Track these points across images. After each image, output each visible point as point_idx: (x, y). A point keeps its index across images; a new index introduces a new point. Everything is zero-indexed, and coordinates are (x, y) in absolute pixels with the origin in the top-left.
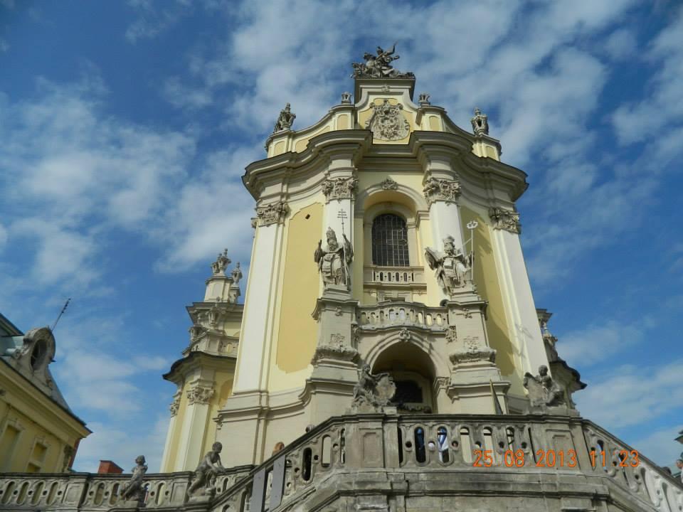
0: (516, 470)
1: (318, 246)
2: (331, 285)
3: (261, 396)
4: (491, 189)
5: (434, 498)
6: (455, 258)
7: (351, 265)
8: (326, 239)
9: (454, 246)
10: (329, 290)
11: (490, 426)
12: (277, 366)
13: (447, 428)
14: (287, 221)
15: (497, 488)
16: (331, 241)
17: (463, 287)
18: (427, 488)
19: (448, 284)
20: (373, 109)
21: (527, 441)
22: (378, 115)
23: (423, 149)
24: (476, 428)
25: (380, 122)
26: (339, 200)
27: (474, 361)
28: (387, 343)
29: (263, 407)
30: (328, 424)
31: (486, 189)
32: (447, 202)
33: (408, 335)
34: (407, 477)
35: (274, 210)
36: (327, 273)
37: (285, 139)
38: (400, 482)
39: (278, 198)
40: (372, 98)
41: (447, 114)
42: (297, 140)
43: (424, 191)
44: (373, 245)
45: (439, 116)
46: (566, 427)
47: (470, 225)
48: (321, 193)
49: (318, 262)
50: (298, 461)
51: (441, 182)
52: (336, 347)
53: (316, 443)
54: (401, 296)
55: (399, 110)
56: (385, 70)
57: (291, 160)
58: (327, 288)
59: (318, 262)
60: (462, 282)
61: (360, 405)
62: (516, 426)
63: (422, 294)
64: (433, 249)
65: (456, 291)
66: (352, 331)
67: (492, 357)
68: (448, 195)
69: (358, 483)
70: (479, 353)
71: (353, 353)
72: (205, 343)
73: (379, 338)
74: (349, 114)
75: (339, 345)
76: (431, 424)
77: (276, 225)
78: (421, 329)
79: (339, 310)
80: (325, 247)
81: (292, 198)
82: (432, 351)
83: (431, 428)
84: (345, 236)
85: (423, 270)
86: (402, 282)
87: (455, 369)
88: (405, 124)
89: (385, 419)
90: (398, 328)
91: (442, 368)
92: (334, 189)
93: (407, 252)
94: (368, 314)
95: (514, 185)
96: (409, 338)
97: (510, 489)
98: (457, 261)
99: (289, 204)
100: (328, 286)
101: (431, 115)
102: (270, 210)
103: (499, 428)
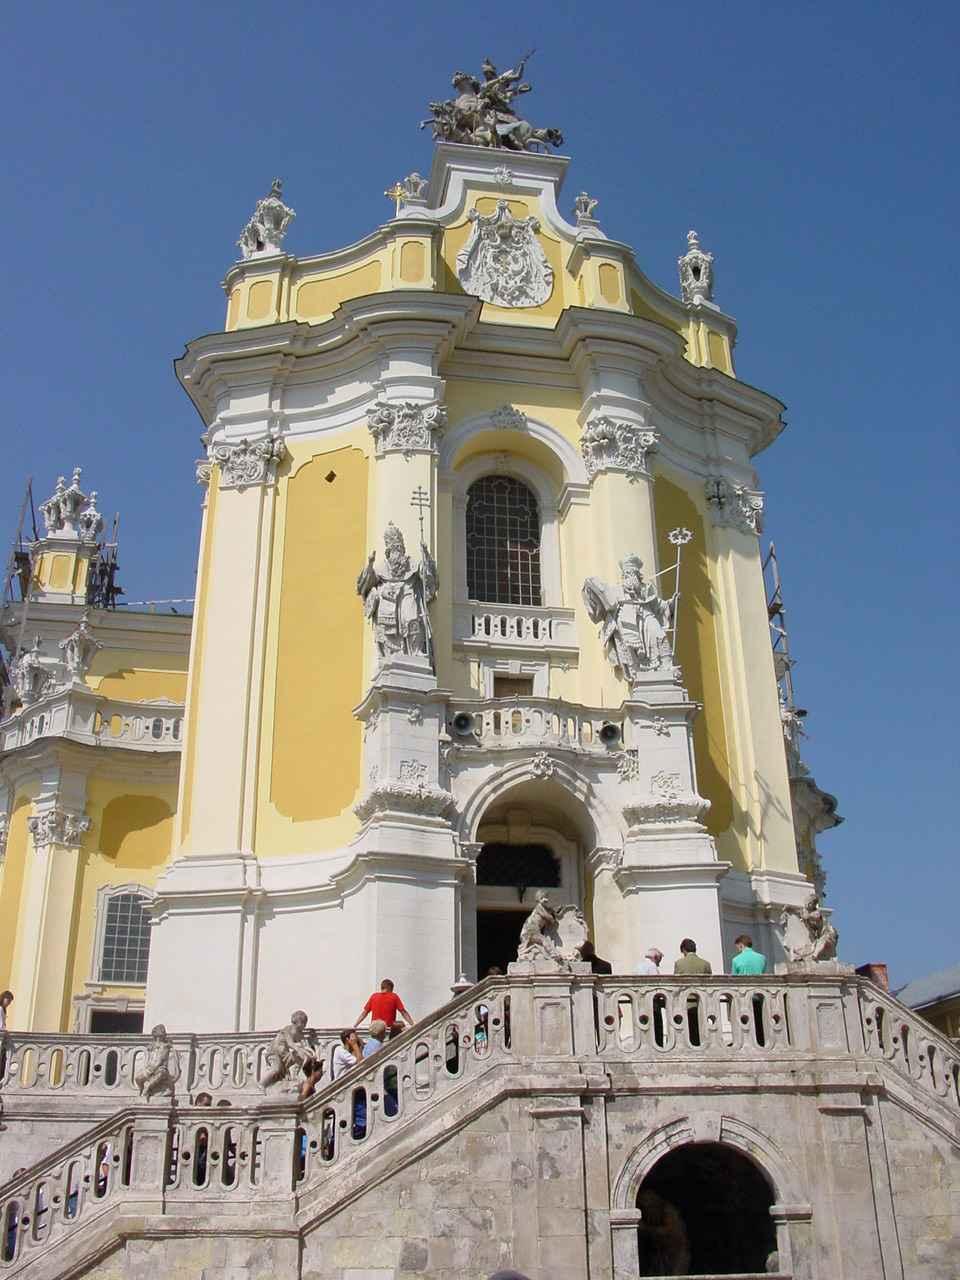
1: (368, 563)
2: (398, 657)
3: (245, 866)
6: (641, 605)
7: (432, 606)
12: (273, 805)
16: (394, 555)
17: (656, 669)
19: (626, 658)
21: (782, 1014)
23: (586, 347)
25: (490, 260)
26: (408, 453)
27: (670, 821)
28: (507, 781)
29: (251, 892)
32: (629, 474)
33: (548, 767)
35: (253, 452)
36: (388, 627)
37: (275, 277)
39: (264, 424)
45: (619, 266)
49: (366, 595)
50: (440, 1047)
51: (620, 427)
52: (411, 787)
54: (527, 670)
55: (532, 233)
57: (294, 339)
58: (385, 661)
60: (654, 657)
63: (568, 668)
65: (641, 677)
66: (441, 754)
67: (704, 816)
68: (632, 459)
70: (679, 805)
71: (445, 800)
72: (63, 714)
73: (491, 769)
74: (427, 242)
76: (643, 990)
78: (573, 752)
79: (416, 711)
80: (381, 567)
81: (294, 427)
82: (591, 798)
84: (425, 548)
85: (572, 615)
86: (528, 640)
87: (632, 834)
88: (545, 271)
90: (530, 751)
91: (609, 833)
92: (395, 427)
93: (536, 568)
95: (759, 428)
96: (550, 772)
98: (646, 613)
100: (390, 659)
101: (605, 261)
102: (244, 451)
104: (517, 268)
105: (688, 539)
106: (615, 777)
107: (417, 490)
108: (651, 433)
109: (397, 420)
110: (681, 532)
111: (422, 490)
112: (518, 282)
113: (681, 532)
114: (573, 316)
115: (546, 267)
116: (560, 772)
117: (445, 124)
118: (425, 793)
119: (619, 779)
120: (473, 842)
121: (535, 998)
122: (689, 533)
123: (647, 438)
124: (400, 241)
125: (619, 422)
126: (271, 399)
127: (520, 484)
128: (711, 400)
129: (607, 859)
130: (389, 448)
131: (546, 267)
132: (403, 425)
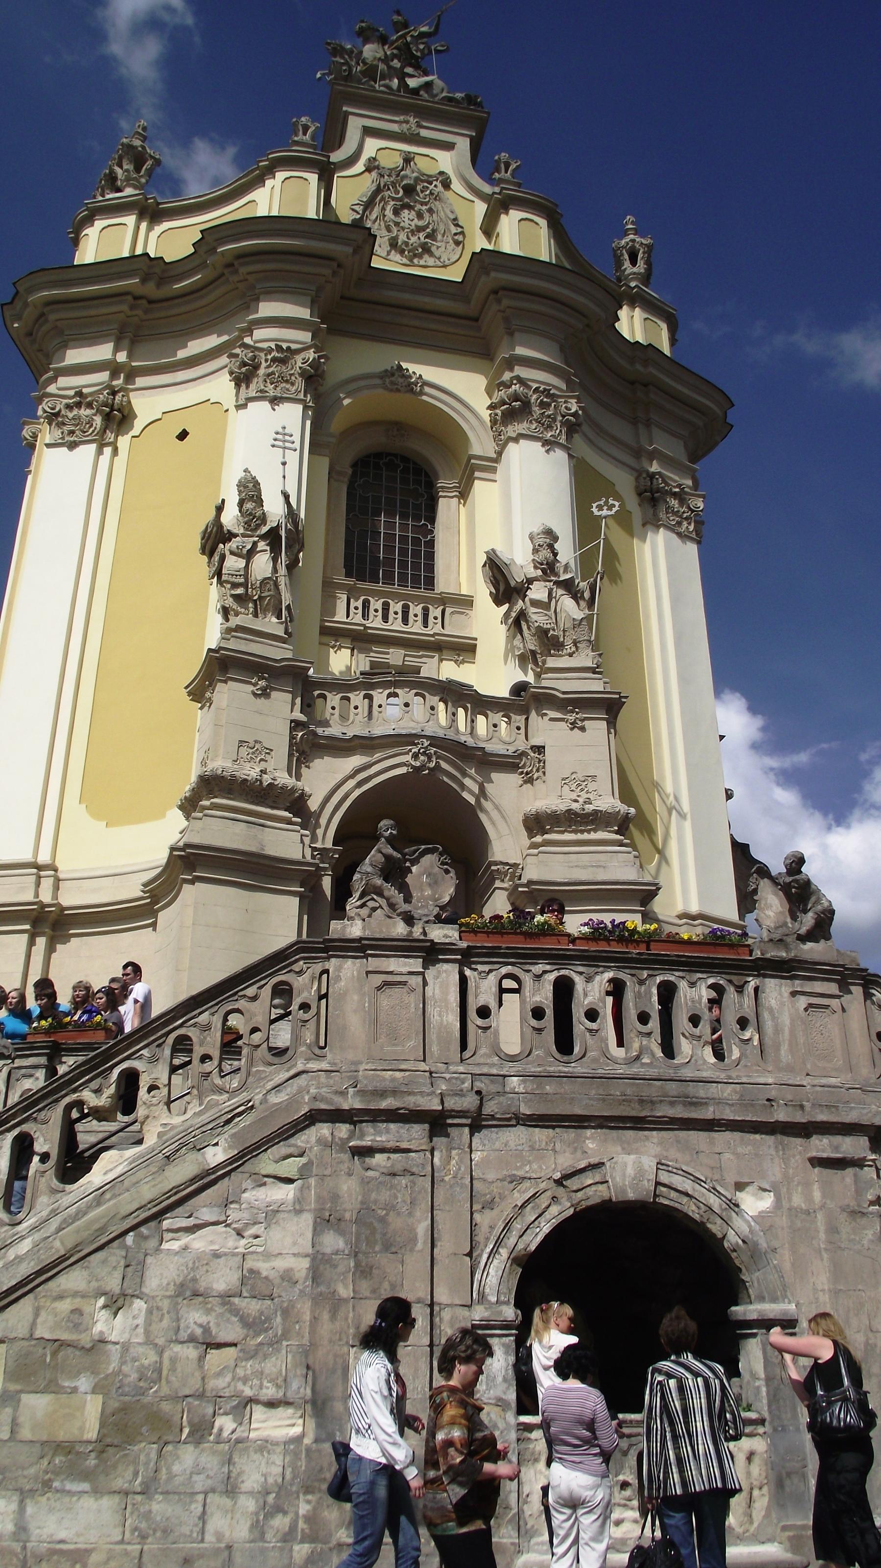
0: (722, 1076)
1: (214, 513)
2: (244, 619)
4: (648, 424)
5: (537, 1130)
6: (556, 583)
7: (296, 570)
8: (236, 499)
9: (555, 555)
10: (239, 628)
11: (672, 978)
13: (577, 979)
14: (124, 442)
15: (679, 1112)
16: (249, 505)
18: (525, 1110)
20: (374, 174)
21: (752, 1017)
22: (387, 193)
24: (641, 982)
25: (389, 212)
26: (275, 401)
30: (287, 958)
31: (634, 422)
34: (478, 1085)
36: (235, 586)
38: (460, 1094)
39: (103, 376)
40: (372, 146)
41: (562, 221)
42: (158, 229)
43: (491, 407)
44: (347, 528)
45: (543, 223)
46: (832, 988)
47: (600, 508)
48: (228, 377)
49: (211, 555)
51: (536, 390)
53: (254, 999)
55: (440, 188)
56: (411, 76)
59: (211, 555)
61: (370, 916)
62: (730, 981)
64: (504, 554)
68: (550, 427)
69: (362, 1093)
73: (357, 761)
75: (258, 770)
77: (93, 447)
78: (463, 745)
80: (230, 518)
81: (140, 382)
83: (538, 977)
84: (286, 497)
88: (454, 230)
89: (432, 953)
92: (262, 371)
94: (334, 699)
97: (708, 1113)
98: (560, 592)
99: (131, 394)
100: (234, 621)
103: (692, 984)
104: (421, 223)
105: (615, 510)
106: (515, 779)
107: (281, 430)
108: (574, 401)
109: (264, 365)
110: (606, 503)
111: (287, 431)
112: (422, 239)
113: (606, 503)
114: (486, 262)
115: (457, 225)
116: (444, 765)
117: (343, 64)
118: (267, 780)
119: (521, 782)
120: (329, 844)
121: (368, 973)
122: (617, 504)
123: (569, 405)
124: (281, 175)
125: (535, 386)
126: (116, 350)
127: (415, 463)
128: (646, 385)
129: (502, 876)
130: (252, 393)
131: (457, 225)
132: (271, 370)
